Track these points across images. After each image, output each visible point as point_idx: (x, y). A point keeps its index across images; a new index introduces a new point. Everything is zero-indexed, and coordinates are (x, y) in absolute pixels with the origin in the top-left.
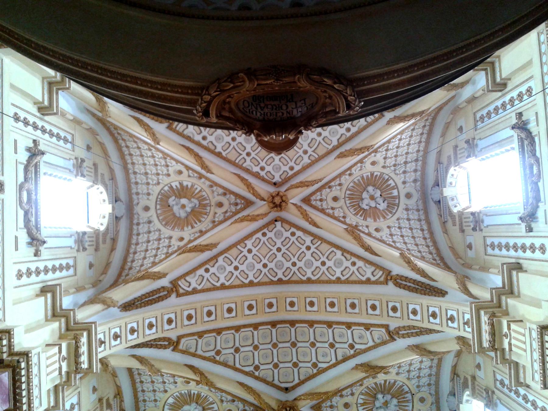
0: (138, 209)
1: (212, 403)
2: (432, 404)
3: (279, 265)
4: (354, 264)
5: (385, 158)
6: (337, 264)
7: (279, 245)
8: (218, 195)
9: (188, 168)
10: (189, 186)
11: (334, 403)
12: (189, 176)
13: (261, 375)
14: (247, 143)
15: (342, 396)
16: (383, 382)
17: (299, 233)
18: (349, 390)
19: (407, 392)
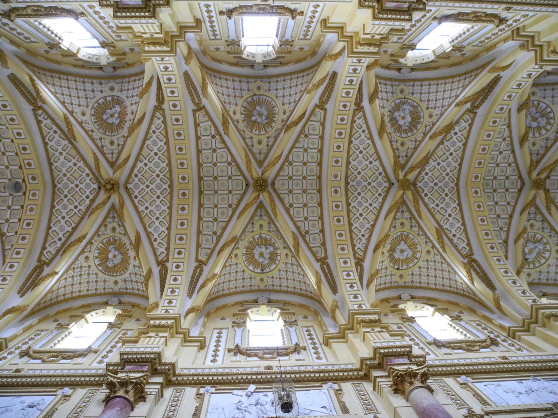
0: (116, 288)
1: (254, 239)
2: (262, 81)
3: (159, 187)
4: (154, 132)
5: (79, 105)
6: (155, 144)
7: (144, 186)
8: (106, 231)
9: (82, 252)
10: (99, 252)
11: (258, 151)
12: (90, 251)
13: (236, 203)
14: (67, 208)
15: (253, 146)
16: (243, 116)
17: (135, 171)
18: (247, 140)
19: (253, 99)
